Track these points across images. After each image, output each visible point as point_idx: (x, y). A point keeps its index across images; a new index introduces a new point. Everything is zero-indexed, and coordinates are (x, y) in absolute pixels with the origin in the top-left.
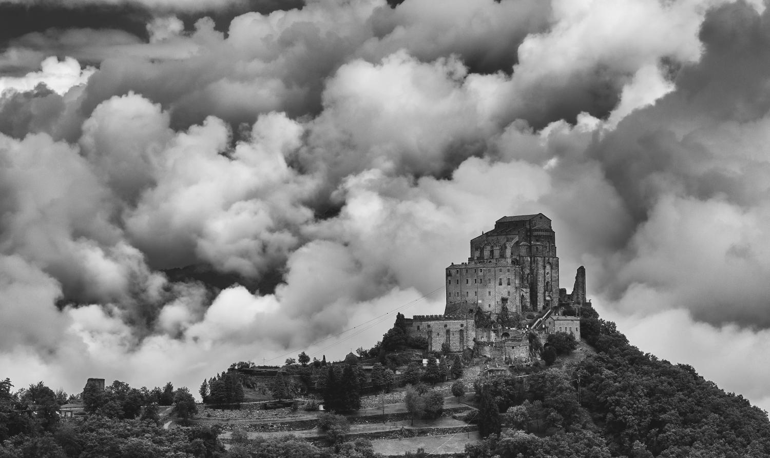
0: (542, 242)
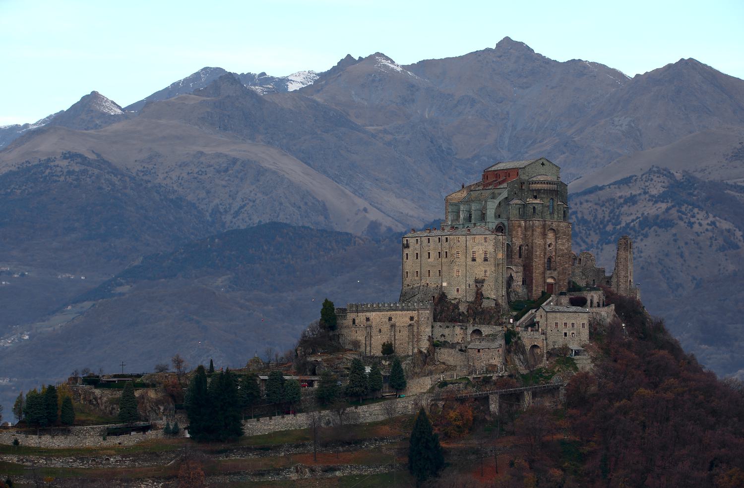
0: (542, 199)
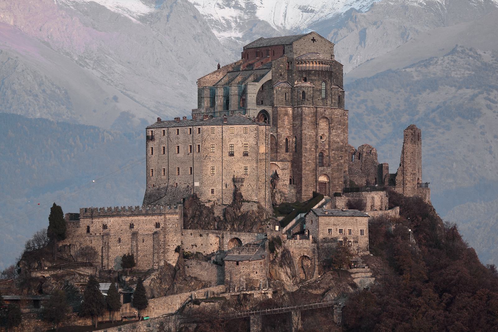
0: (312, 81)
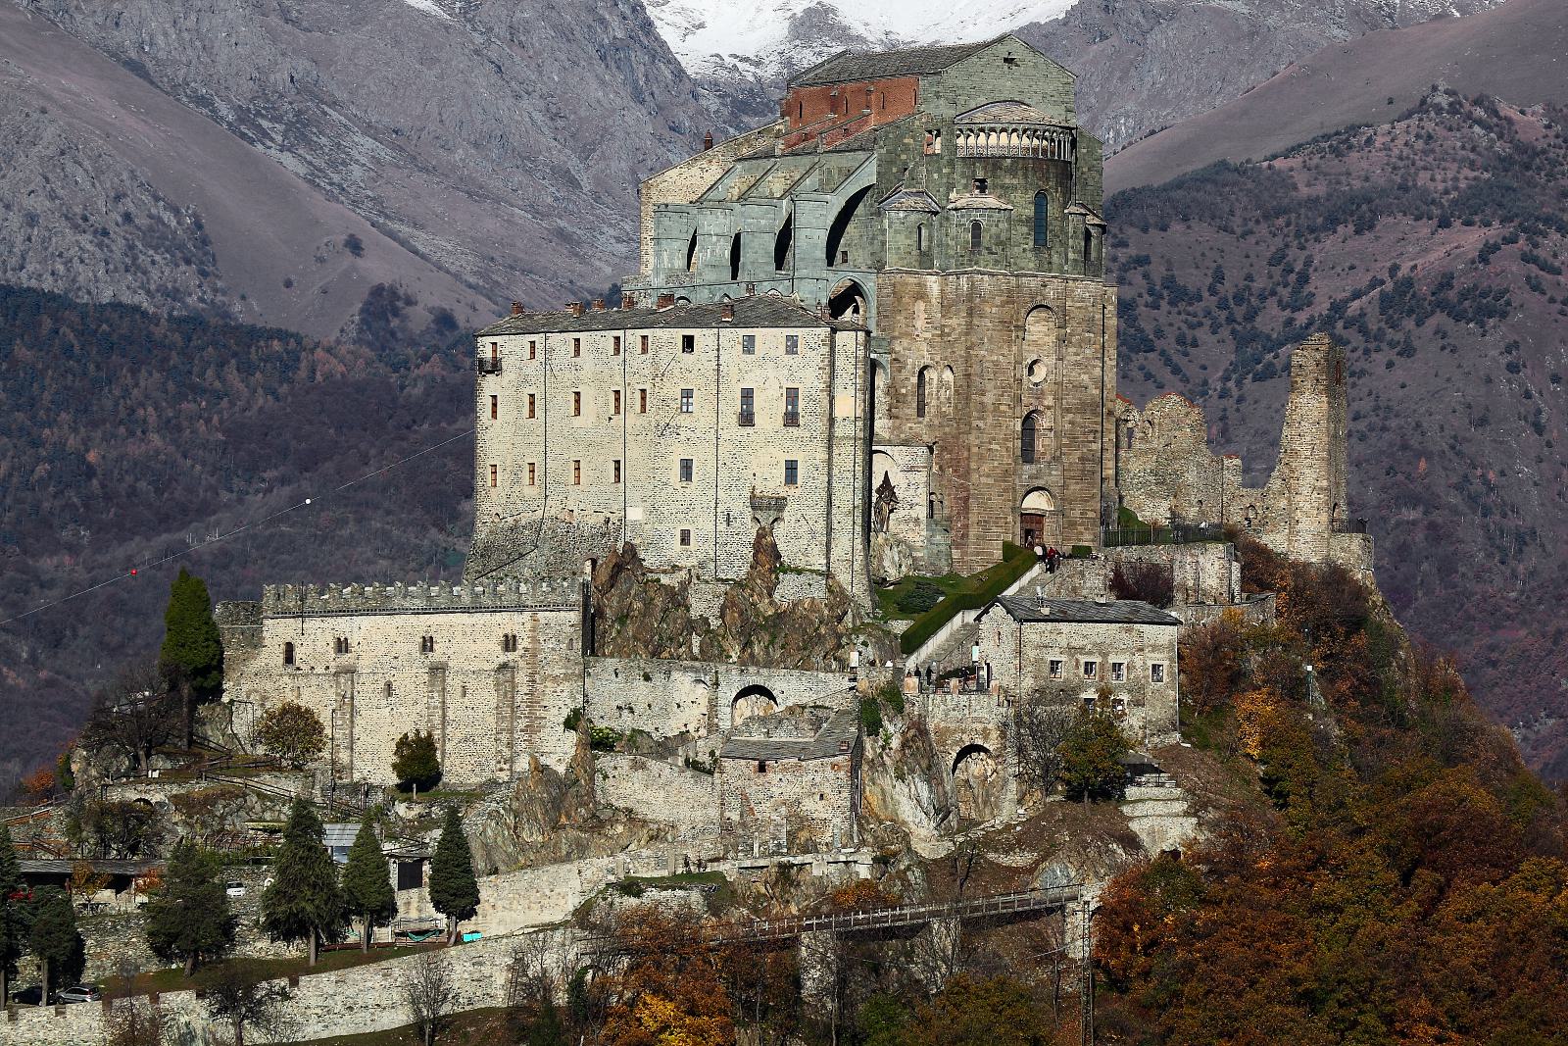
0: (1005, 191)
